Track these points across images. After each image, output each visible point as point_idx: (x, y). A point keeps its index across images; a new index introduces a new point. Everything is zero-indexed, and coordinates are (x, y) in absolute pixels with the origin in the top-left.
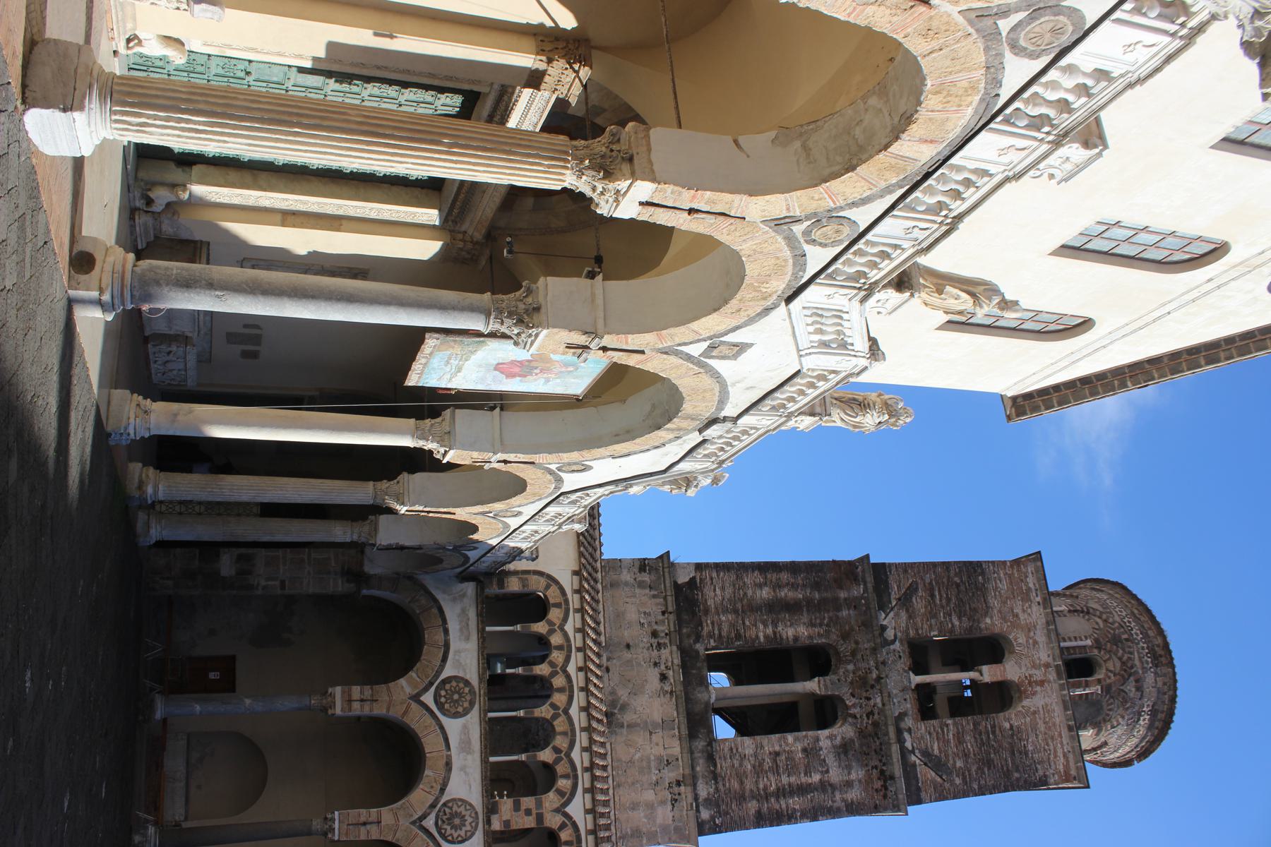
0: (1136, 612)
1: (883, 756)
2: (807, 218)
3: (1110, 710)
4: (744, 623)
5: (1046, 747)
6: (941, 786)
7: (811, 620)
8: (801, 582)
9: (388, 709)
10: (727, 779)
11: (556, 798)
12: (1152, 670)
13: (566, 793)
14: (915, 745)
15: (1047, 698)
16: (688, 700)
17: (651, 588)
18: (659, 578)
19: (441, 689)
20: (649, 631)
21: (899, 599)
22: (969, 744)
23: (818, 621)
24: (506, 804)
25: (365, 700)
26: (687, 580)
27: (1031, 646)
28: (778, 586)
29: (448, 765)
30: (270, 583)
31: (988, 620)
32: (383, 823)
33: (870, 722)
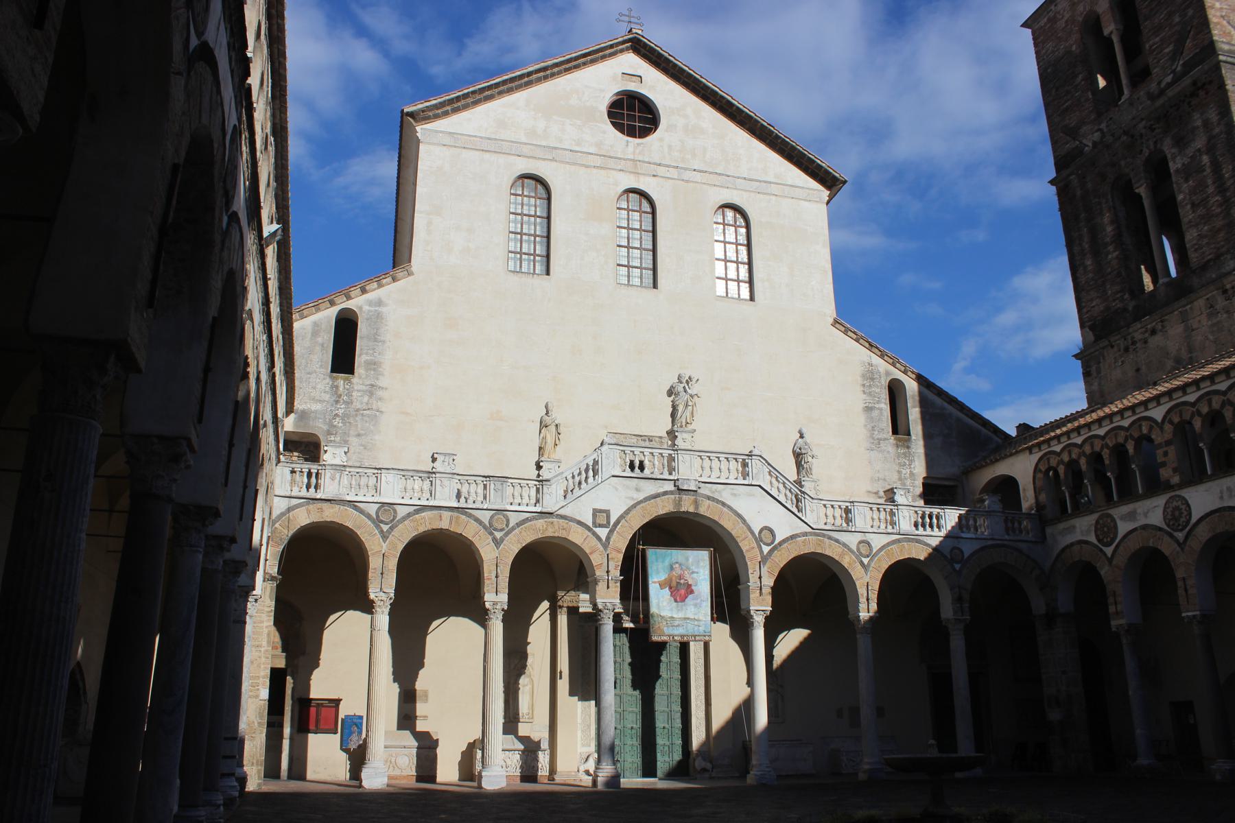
2: (491, 534)
4: (1110, 273)
13: (1151, 425)
14: (1169, 72)
17: (1099, 362)
26: (1091, 333)
29: (1145, 527)
32: (1185, 576)
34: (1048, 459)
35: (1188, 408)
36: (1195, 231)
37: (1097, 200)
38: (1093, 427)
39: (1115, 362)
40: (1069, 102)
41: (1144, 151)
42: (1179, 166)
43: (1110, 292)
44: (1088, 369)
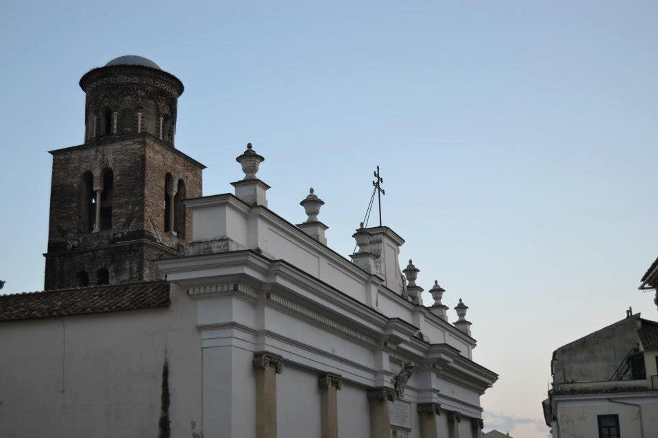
31: (75, 185)
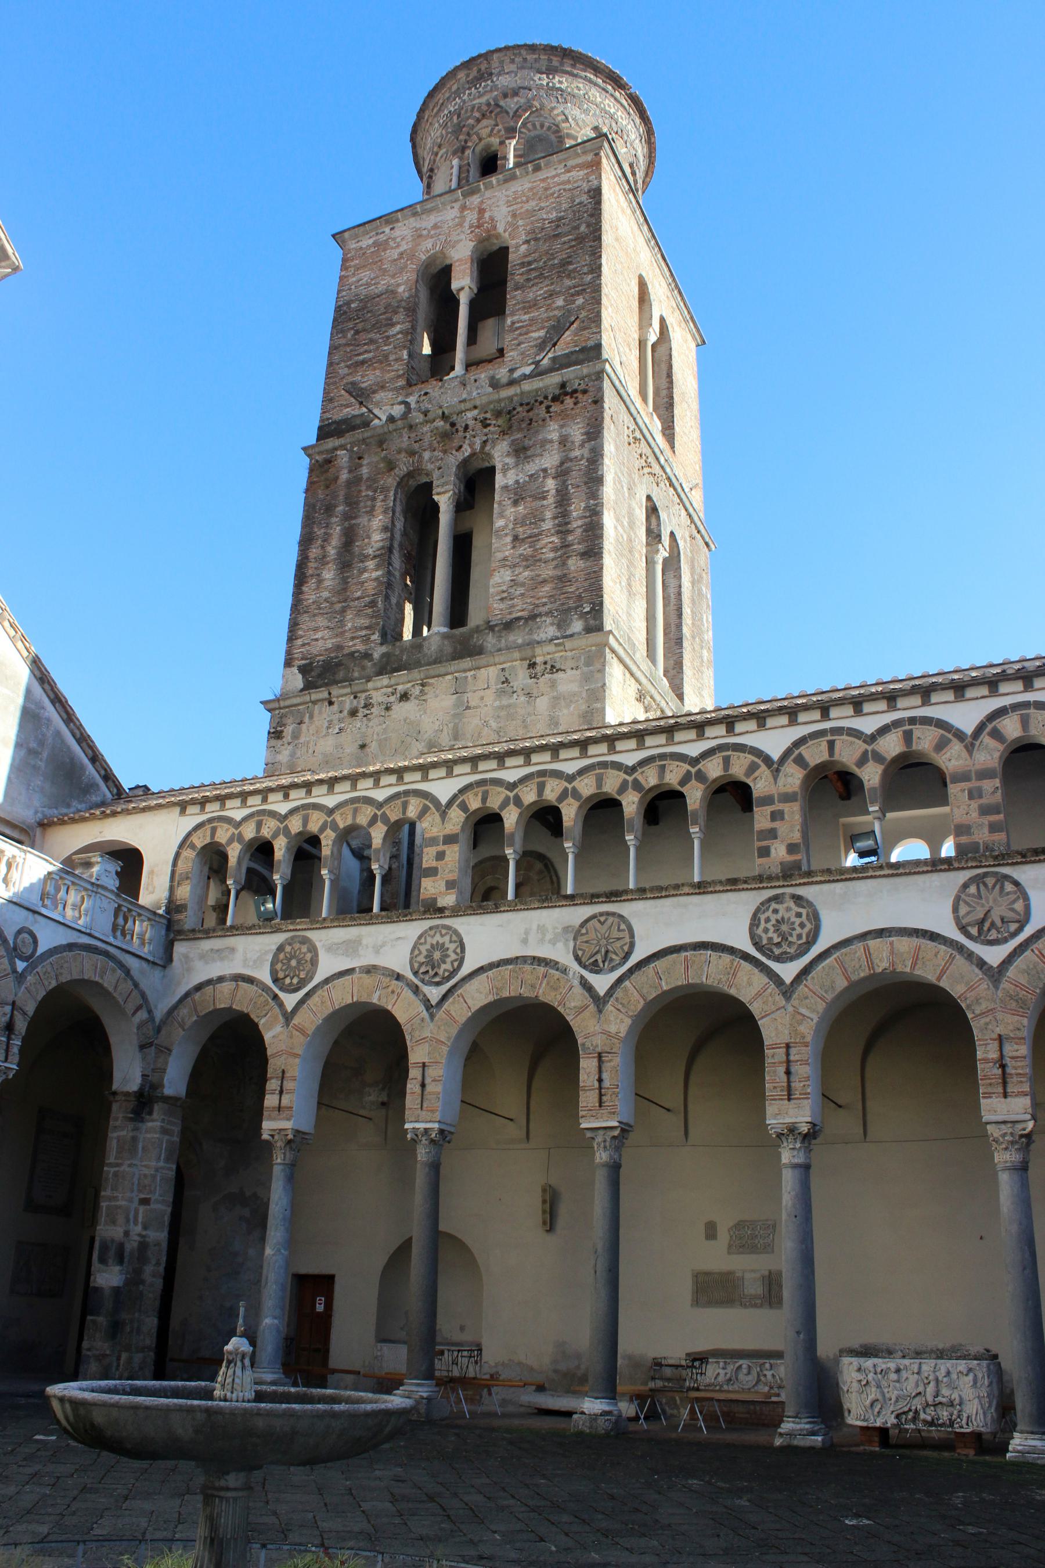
0: (435, 111)
1: (536, 401)
3: (542, 126)
4: (358, 598)
5: (555, 195)
6: (583, 322)
7: (367, 512)
8: (323, 531)
9: (296, 1055)
10: (537, 602)
11: (429, 819)
12: (495, 79)
13: (425, 805)
14: (530, 361)
15: (501, 203)
16: (437, 661)
18: (291, 712)
19: (284, 984)
20: (349, 720)
21: (361, 403)
22: (539, 293)
23: (369, 503)
24: (429, 887)
25: (281, 1087)
26: (300, 676)
27: (438, 231)
28: (323, 560)
29: (370, 970)
30: (140, 1220)
32: (426, 1060)
33: (494, 422)
34: (214, 830)
35: (502, 790)
36: (509, 573)
37: (370, 493)
38: (316, 791)
39: (328, 728)
40: (371, 355)
41: (463, 449)
42: (511, 482)
43: (349, 625)
44: (279, 729)
